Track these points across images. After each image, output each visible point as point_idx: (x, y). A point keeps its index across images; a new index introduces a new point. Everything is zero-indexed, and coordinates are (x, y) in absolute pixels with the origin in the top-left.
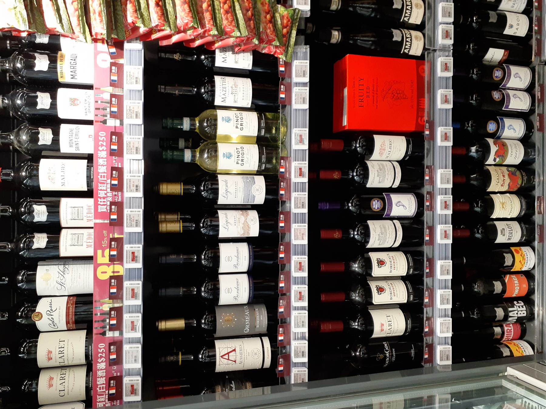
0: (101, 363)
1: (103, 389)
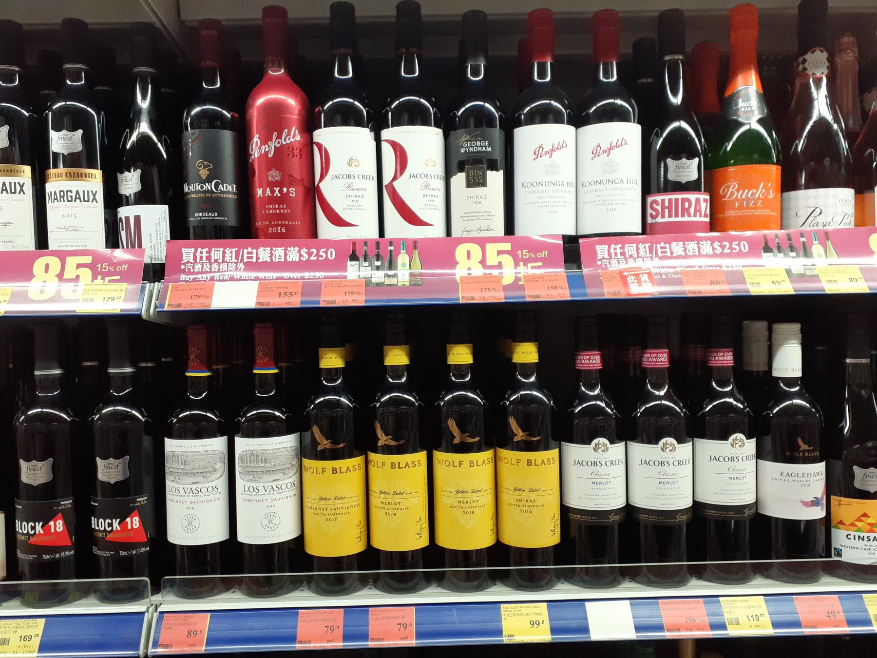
0: (298, 254)
1: (248, 258)
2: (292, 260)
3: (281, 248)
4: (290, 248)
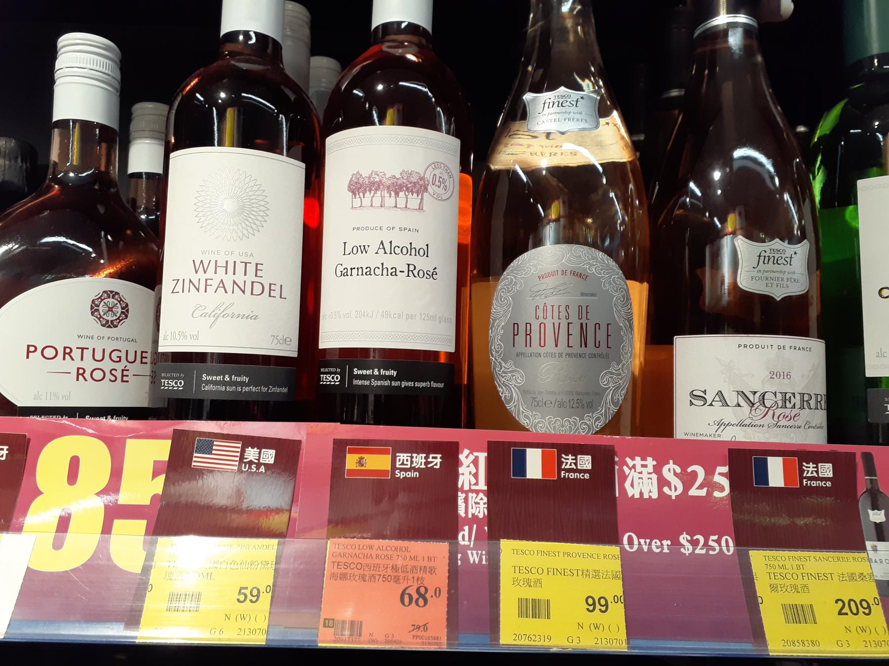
0: (654, 477)
2: (641, 494)
4: (633, 459)
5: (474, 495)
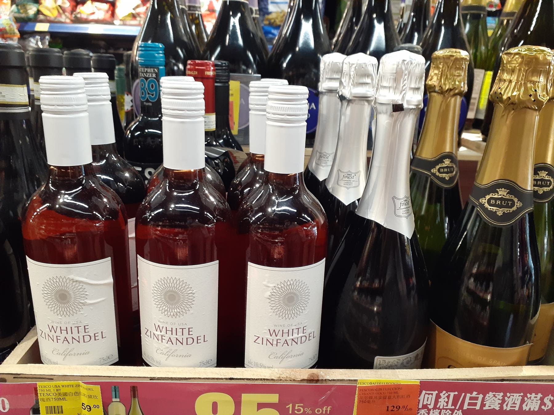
0: (539, 402)
1: (469, 404)
2: (530, 409)
3: (518, 395)
4: (531, 394)
5: (445, 410)
